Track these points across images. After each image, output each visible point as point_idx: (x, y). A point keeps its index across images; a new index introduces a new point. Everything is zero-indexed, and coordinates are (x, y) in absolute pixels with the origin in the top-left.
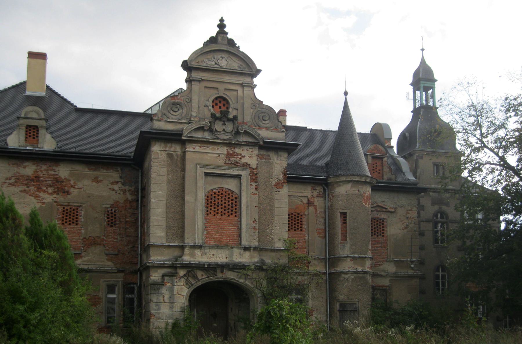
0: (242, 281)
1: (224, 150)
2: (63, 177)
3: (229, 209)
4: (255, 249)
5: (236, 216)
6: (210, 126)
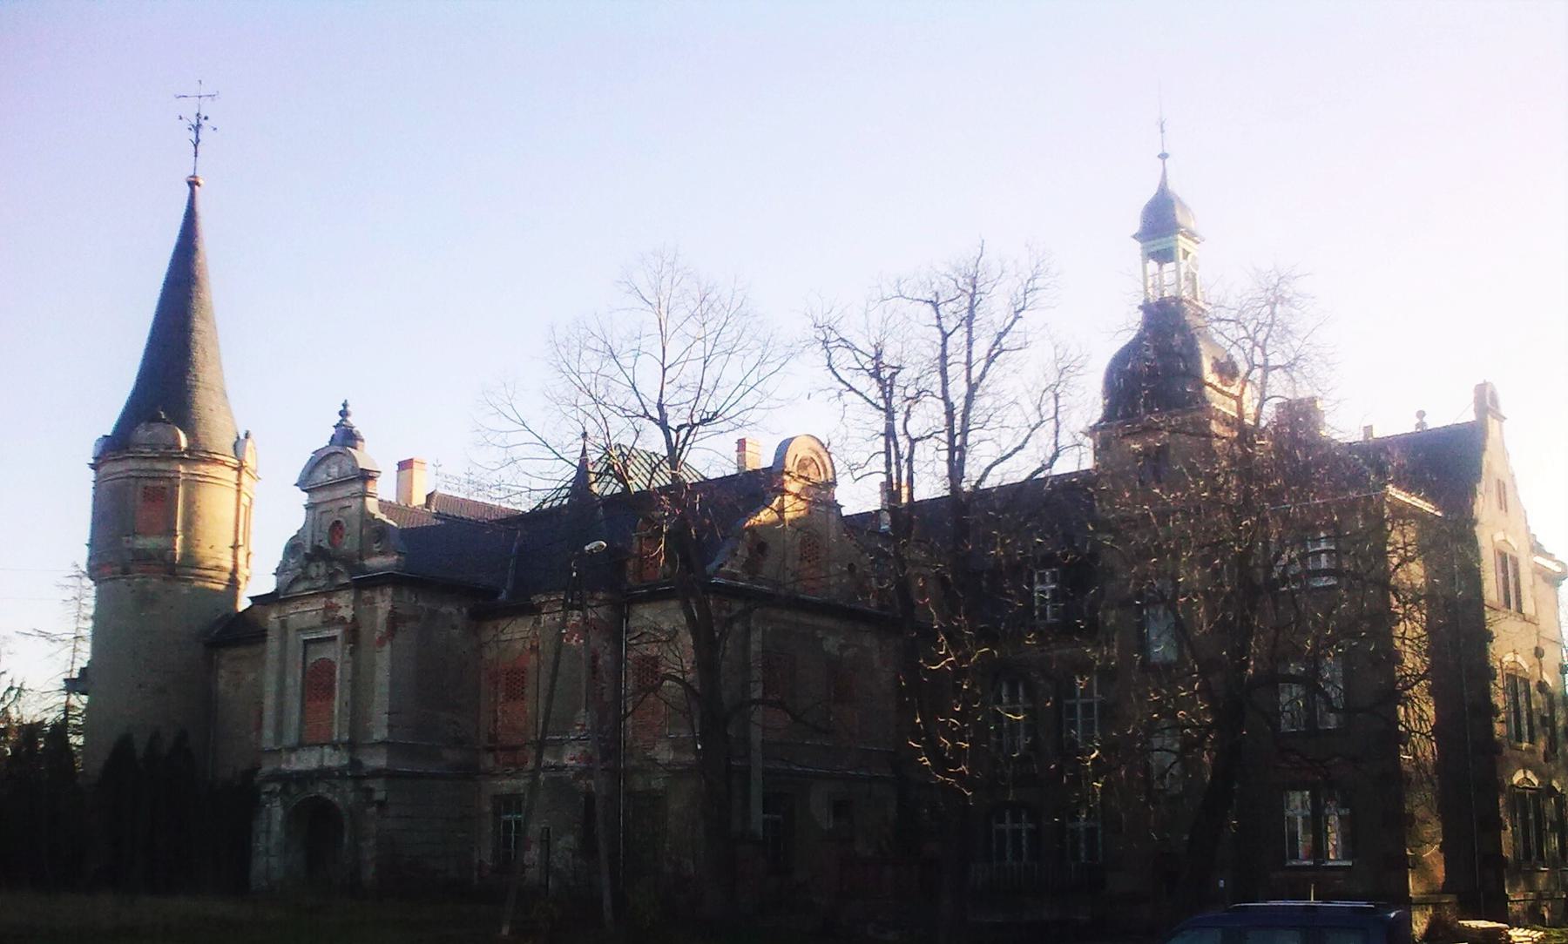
1: (320, 604)
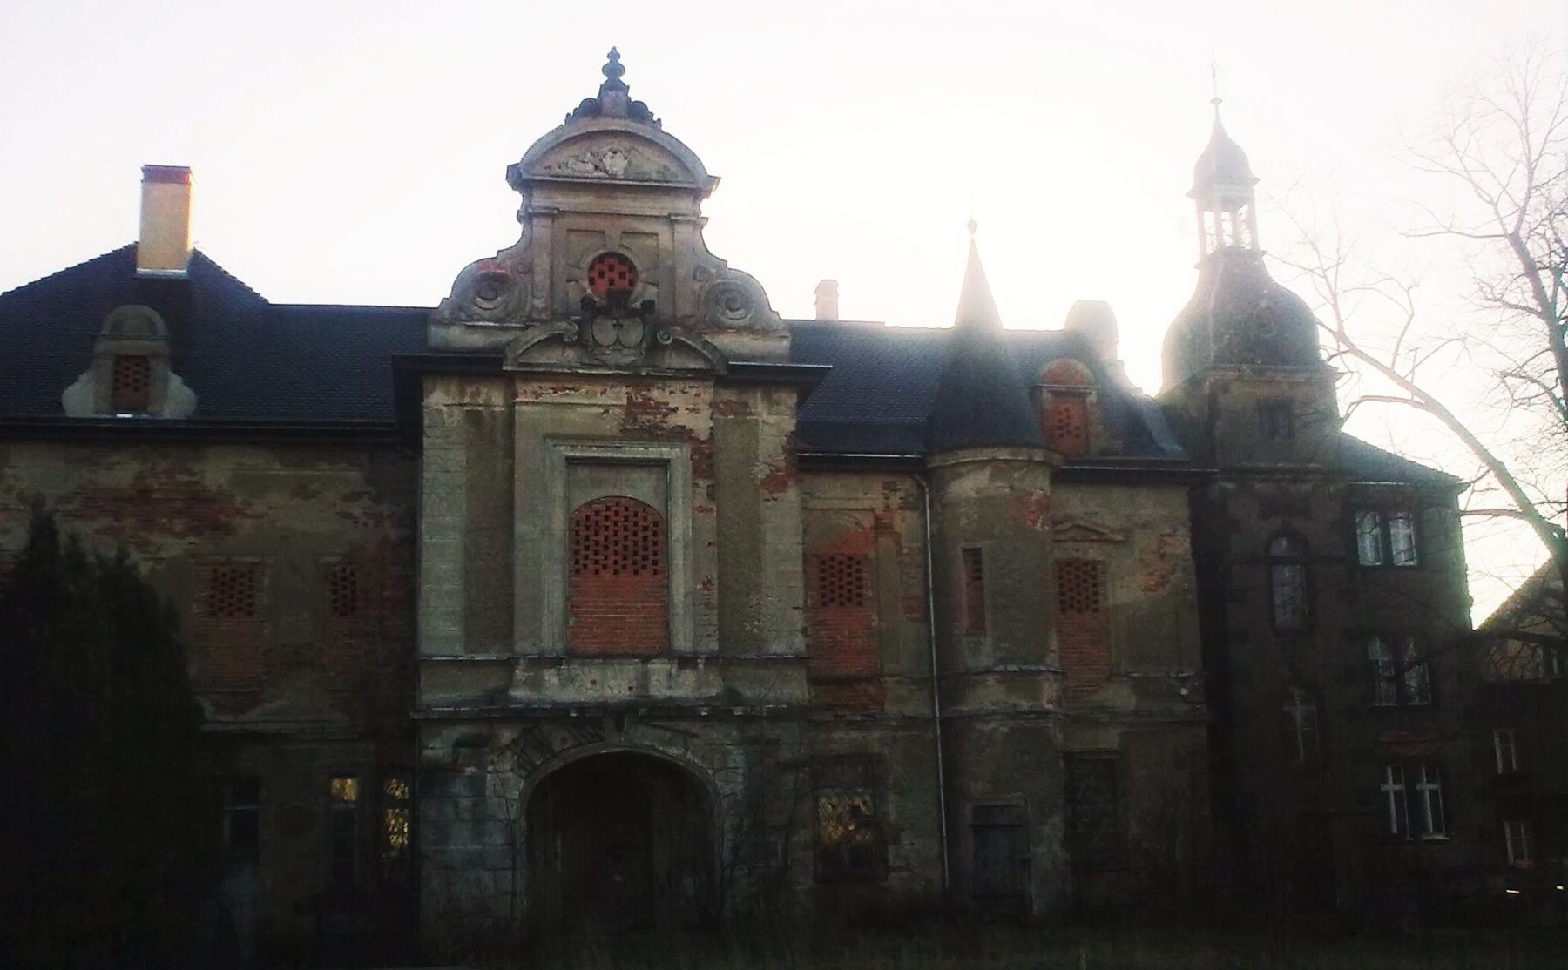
0: (674, 751)
1: (618, 396)
2: (214, 488)
3: (636, 554)
4: (711, 660)
5: (655, 572)
6: (579, 334)
